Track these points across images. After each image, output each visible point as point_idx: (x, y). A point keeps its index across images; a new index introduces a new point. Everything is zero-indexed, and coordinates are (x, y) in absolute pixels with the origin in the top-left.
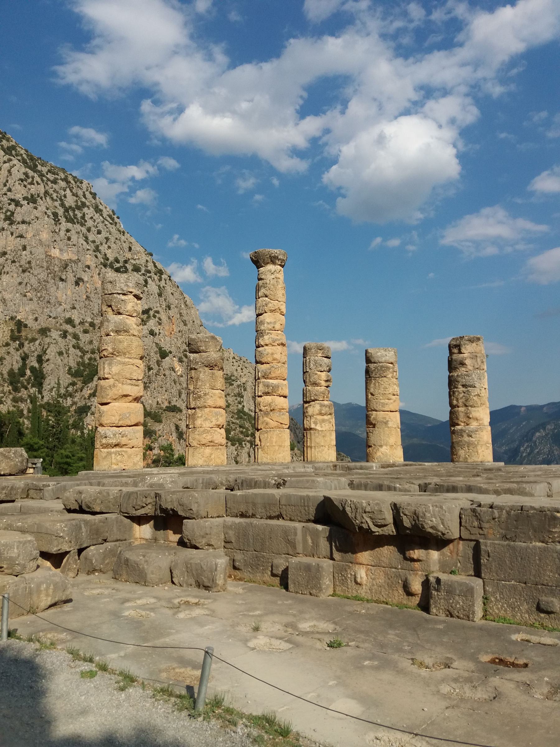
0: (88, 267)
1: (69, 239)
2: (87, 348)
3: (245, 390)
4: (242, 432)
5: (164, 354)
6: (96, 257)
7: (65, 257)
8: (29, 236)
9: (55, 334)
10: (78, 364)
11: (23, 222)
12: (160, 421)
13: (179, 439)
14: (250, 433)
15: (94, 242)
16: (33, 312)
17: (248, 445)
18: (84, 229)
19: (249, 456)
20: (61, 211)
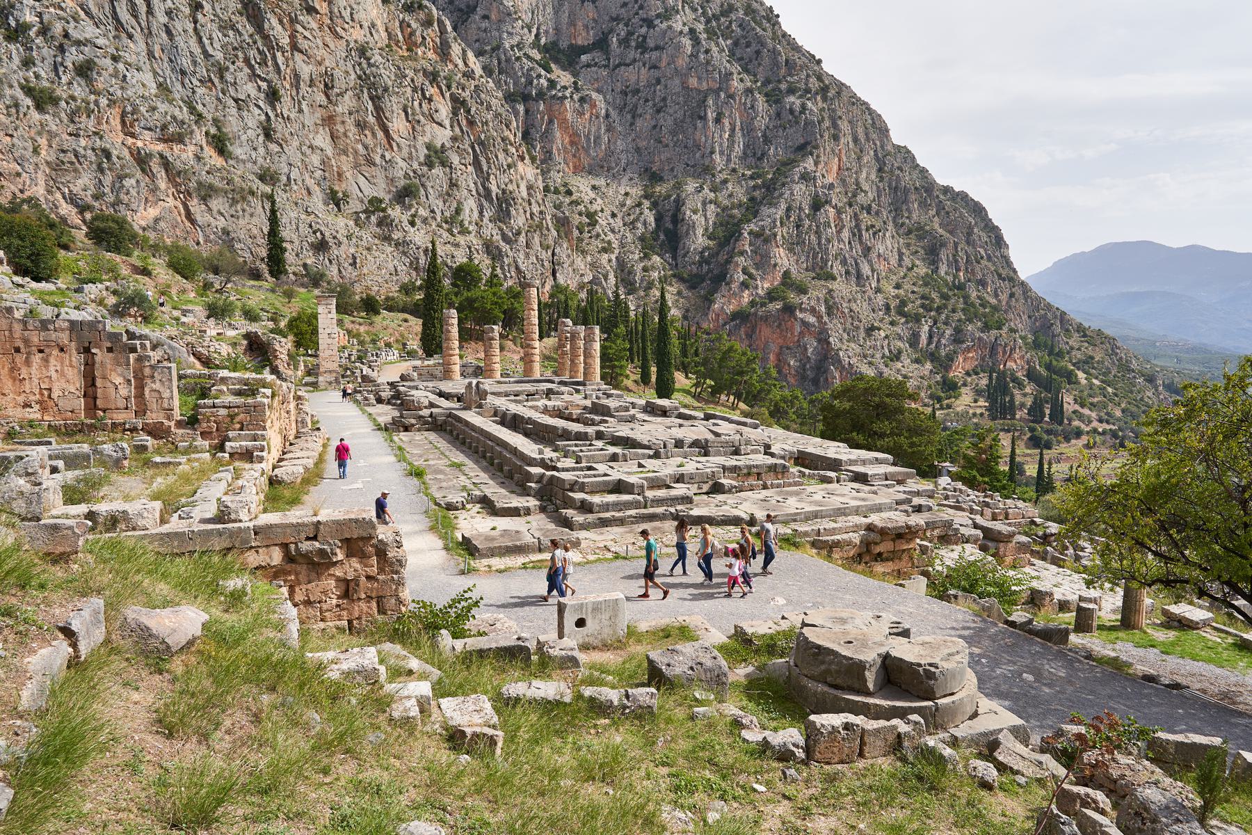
0: (731, 96)
1: (708, 63)
2: (726, 202)
3: (943, 245)
4: (923, 306)
5: (817, 205)
6: (742, 80)
7: (704, 86)
8: (663, 64)
9: (691, 186)
10: (715, 223)
11: (657, 48)
15: (741, 59)
16: (669, 160)
17: (930, 322)
18: (729, 42)
19: (931, 337)
20: (700, 27)
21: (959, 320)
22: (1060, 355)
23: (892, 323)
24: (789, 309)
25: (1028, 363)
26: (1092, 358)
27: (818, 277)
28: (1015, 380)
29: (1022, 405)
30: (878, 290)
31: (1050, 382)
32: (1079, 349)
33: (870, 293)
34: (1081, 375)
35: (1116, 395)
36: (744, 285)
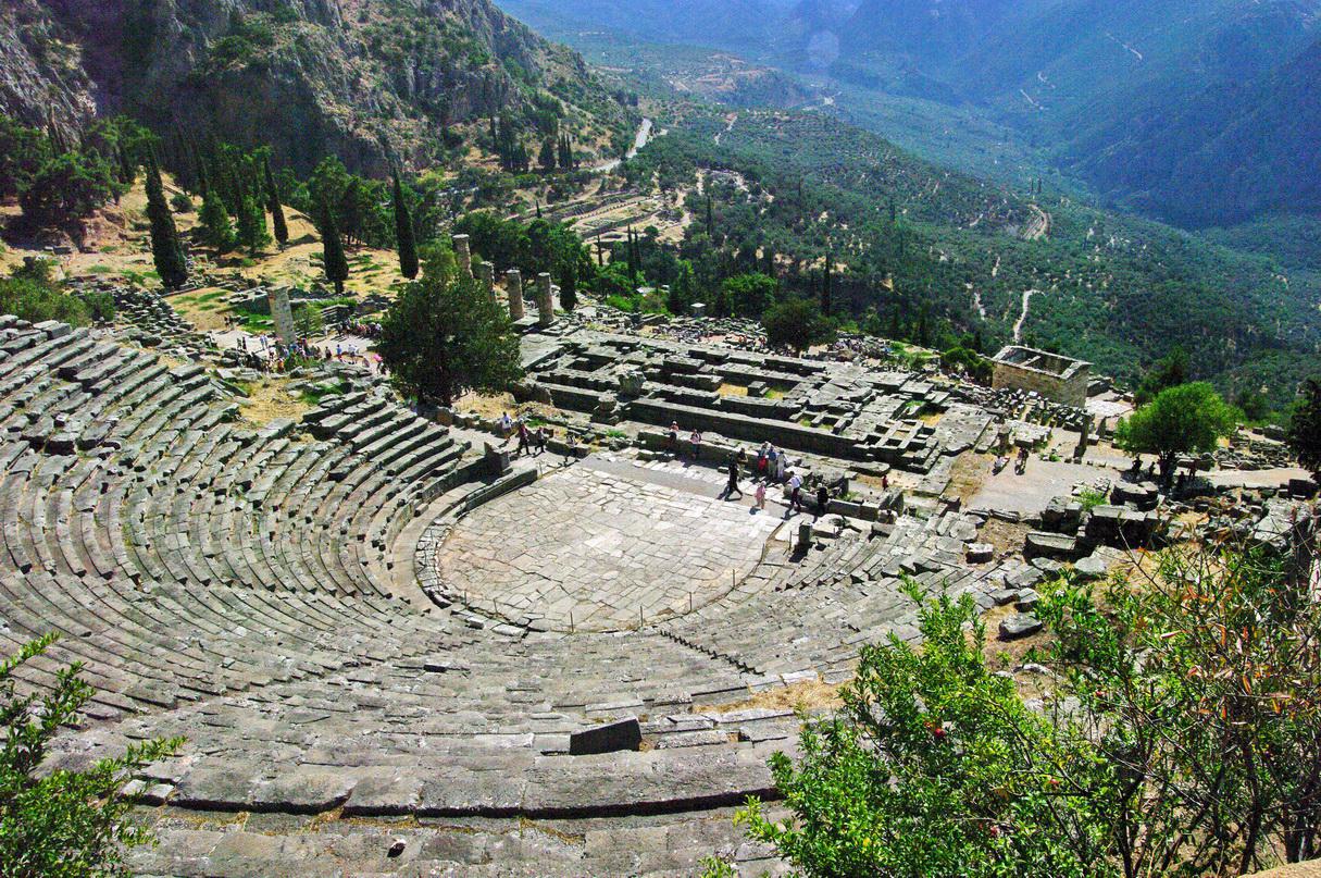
12: (271, 43)
13: (307, 68)
14: (413, 41)
21: (445, 58)
22: (534, 80)
23: (374, 70)
24: (258, 68)
25: (520, 100)
26: (563, 79)
27: (279, 20)
28: (514, 123)
29: (531, 152)
30: (346, 27)
31: (544, 119)
32: (549, 70)
33: (340, 32)
34: (563, 104)
35: (596, 121)
36: (185, 37)
